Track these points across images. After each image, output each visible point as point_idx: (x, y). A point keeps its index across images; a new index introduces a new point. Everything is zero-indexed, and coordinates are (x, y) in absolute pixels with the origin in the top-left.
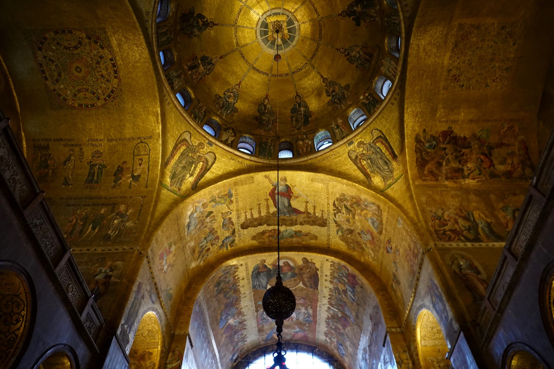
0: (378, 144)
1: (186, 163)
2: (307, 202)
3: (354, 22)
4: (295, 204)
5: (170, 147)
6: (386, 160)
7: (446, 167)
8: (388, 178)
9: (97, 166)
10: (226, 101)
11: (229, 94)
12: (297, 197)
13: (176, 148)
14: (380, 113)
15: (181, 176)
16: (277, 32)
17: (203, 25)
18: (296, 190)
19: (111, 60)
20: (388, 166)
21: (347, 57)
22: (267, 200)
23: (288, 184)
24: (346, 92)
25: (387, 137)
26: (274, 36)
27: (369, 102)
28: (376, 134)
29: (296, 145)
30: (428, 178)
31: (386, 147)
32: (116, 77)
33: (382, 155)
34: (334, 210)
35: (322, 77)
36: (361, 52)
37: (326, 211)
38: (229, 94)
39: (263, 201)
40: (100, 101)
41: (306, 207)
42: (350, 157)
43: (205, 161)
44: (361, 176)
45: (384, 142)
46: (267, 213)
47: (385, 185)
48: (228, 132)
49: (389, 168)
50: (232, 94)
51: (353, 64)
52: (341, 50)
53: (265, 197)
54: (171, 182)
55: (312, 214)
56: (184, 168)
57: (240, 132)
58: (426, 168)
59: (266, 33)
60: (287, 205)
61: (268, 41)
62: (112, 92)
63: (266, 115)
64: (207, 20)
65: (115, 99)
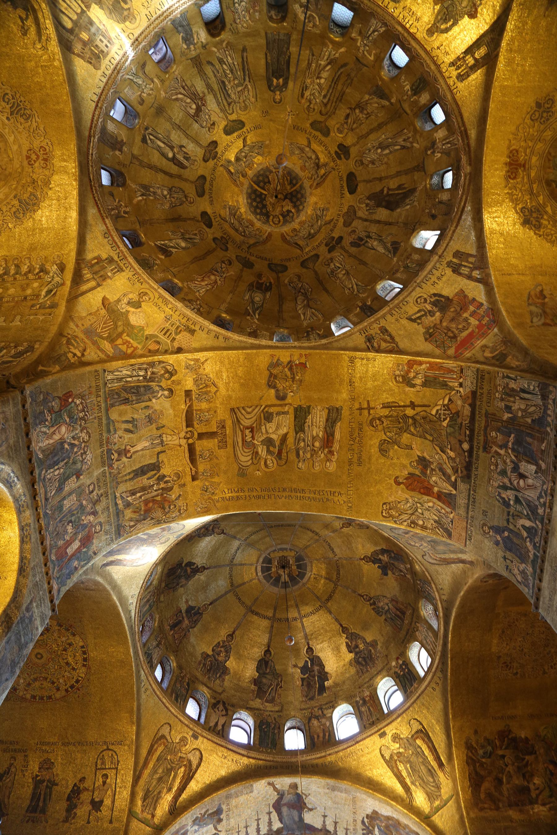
0: (419, 742)
1: (163, 772)
2: (325, 816)
3: (380, 571)
4: (309, 818)
5: (144, 752)
6: (430, 767)
7: (508, 786)
8: (435, 797)
9: (45, 784)
10: (215, 660)
11: (219, 649)
12: (311, 810)
13: (150, 752)
14: (418, 697)
15: (155, 793)
16: (283, 567)
17: (191, 572)
18: (310, 801)
19: (82, 647)
20: (433, 778)
21: (372, 607)
22: (269, 813)
23: (299, 791)
24: (373, 651)
25: (430, 734)
26: (279, 572)
27: (404, 675)
28: (416, 726)
29: (309, 727)
30: (486, 806)
31: (429, 747)
32: (84, 665)
33: (424, 759)
34: (363, 830)
35: (341, 625)
36: (390, 605)
37: (352, 830)
38: (219, 649)
39: (264, 814)
40: (59, 693)
41: (324, 822)
42: (382, 756)
43: (188, 765)
44: (399, 789)
45: (426, 739)
46: (268, 831)
47: (431, 809)
48: (218, 709)
49: (434, 781)
50: (222, 649)
51: (381, 616)
52: (365, 597)
53: (267, 811)
54: (143, 806)
55: (332, 832)
56: (160, 779)
57: (233, 706)
58: (482, 789)
59: (269, 569)
60: (297, 819)
61: (272, 578)
62: (77, 681)
63: (267, 676)
64: (197, 566)
65: (79, 690)
